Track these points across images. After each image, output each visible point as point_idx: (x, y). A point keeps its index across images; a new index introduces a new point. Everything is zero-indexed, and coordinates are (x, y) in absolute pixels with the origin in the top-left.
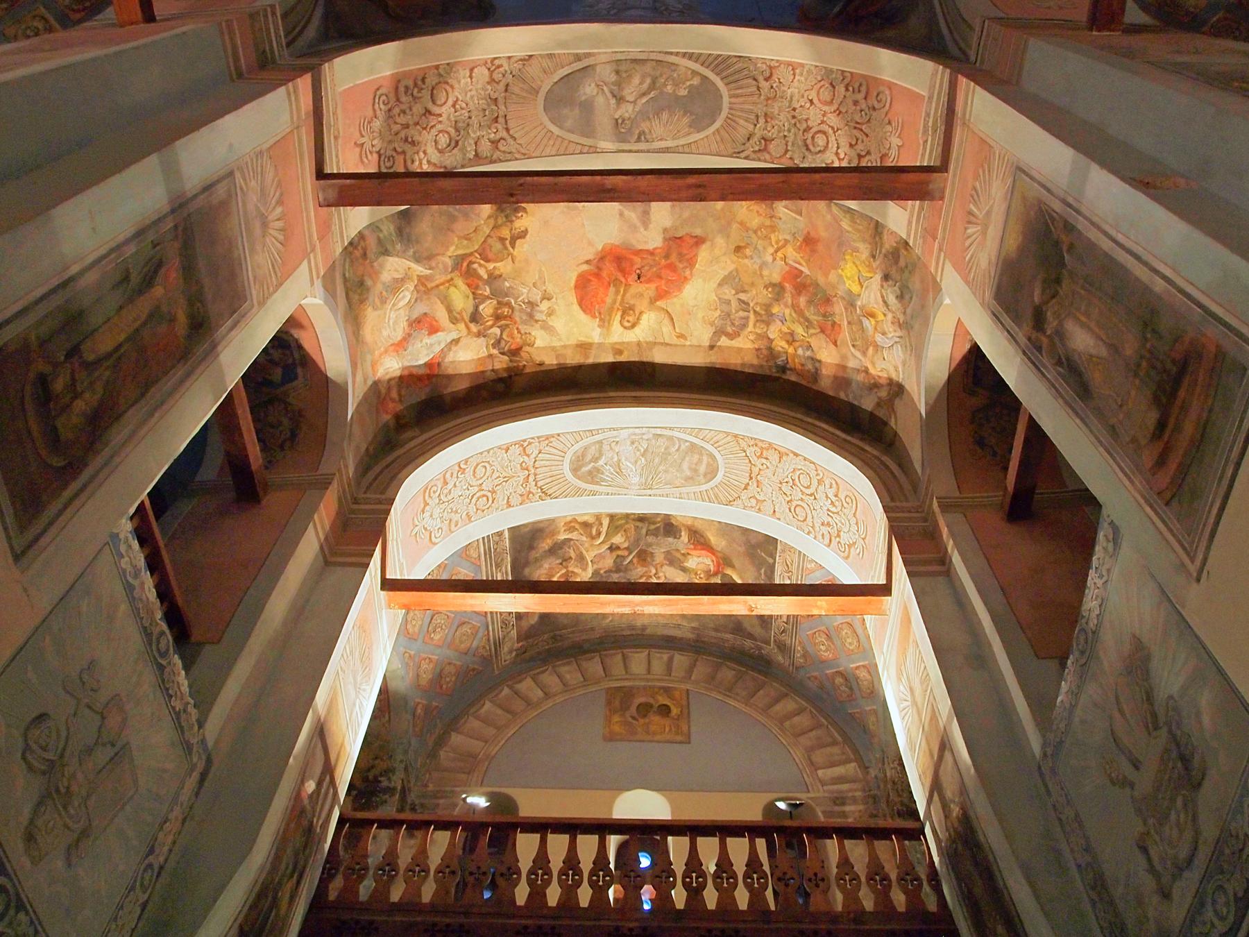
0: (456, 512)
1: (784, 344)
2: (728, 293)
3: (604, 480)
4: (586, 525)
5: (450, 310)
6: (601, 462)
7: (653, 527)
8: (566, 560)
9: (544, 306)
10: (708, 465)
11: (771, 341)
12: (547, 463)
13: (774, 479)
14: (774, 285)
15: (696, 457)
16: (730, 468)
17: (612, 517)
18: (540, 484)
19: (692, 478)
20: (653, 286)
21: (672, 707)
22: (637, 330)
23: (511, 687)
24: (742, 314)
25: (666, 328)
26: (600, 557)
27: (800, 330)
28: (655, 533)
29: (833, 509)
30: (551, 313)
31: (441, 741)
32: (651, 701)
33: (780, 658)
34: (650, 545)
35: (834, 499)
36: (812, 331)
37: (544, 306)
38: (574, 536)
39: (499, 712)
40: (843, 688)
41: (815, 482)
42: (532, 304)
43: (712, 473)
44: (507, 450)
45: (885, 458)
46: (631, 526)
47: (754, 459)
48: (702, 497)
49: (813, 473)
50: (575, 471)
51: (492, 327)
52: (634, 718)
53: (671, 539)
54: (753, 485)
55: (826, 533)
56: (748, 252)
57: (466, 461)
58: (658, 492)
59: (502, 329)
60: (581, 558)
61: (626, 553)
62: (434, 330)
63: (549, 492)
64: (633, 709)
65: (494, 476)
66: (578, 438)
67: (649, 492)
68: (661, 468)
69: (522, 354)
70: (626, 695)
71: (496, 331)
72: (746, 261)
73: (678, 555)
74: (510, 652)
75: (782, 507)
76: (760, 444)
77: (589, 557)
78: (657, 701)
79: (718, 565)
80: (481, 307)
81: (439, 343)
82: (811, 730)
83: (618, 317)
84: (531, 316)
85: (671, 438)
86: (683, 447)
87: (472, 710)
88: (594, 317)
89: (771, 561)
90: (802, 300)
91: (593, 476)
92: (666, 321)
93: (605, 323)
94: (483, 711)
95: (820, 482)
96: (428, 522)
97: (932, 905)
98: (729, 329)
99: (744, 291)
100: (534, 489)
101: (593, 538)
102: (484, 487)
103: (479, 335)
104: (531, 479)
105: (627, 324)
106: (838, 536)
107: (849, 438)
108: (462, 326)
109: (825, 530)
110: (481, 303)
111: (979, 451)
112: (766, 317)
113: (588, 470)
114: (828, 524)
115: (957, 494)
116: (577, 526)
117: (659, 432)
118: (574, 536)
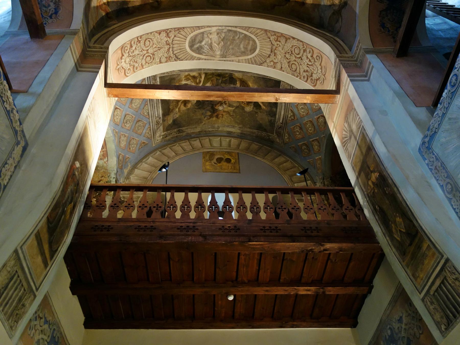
0: (136, 62)
3: (205, 53)
4: (194, 77)
6: (203, 43)
7: (224, 79)
10: (252, 45)
12: (178, 42)
15: (247, 41)
16: (262, 47)
18: (175, 52)
19: (244, 52)
21: (232, 159)
23: (160, 152)
28: (225, 82)
29: (310, 63)
32: (222, 157)
33: (278, 140)
35: (310, 58)
40: (306, 150)
41: (302, 51)
43: (254, 49)
44: (160, 33)
45: (336, 38)
46: (214, 78)
47: (274, 42)
50: (191, 47)
52: (215, 163)
63: (179, 57)
64: (215, 160)
65: (155, 46)
66: (193, 30)
67: (224, 59)
68: (231, 47)
70: (212, 155)
74: (160, 136)
75: (285, 65)
76: (277, 34)
78: (225, 157)
85: (235, 32)
86: (241, 36)
87: (144, 160)
91: (199, 50)
94: (148, 161)
95: (304, 51)
96: (123, 64)
100: (172, 55)
102: (149, 51)
104: (171, 50)
106: (312, 76)
109: (305, 74)
111: (382, 29)
116: (190, 78)
117: (230, 28)
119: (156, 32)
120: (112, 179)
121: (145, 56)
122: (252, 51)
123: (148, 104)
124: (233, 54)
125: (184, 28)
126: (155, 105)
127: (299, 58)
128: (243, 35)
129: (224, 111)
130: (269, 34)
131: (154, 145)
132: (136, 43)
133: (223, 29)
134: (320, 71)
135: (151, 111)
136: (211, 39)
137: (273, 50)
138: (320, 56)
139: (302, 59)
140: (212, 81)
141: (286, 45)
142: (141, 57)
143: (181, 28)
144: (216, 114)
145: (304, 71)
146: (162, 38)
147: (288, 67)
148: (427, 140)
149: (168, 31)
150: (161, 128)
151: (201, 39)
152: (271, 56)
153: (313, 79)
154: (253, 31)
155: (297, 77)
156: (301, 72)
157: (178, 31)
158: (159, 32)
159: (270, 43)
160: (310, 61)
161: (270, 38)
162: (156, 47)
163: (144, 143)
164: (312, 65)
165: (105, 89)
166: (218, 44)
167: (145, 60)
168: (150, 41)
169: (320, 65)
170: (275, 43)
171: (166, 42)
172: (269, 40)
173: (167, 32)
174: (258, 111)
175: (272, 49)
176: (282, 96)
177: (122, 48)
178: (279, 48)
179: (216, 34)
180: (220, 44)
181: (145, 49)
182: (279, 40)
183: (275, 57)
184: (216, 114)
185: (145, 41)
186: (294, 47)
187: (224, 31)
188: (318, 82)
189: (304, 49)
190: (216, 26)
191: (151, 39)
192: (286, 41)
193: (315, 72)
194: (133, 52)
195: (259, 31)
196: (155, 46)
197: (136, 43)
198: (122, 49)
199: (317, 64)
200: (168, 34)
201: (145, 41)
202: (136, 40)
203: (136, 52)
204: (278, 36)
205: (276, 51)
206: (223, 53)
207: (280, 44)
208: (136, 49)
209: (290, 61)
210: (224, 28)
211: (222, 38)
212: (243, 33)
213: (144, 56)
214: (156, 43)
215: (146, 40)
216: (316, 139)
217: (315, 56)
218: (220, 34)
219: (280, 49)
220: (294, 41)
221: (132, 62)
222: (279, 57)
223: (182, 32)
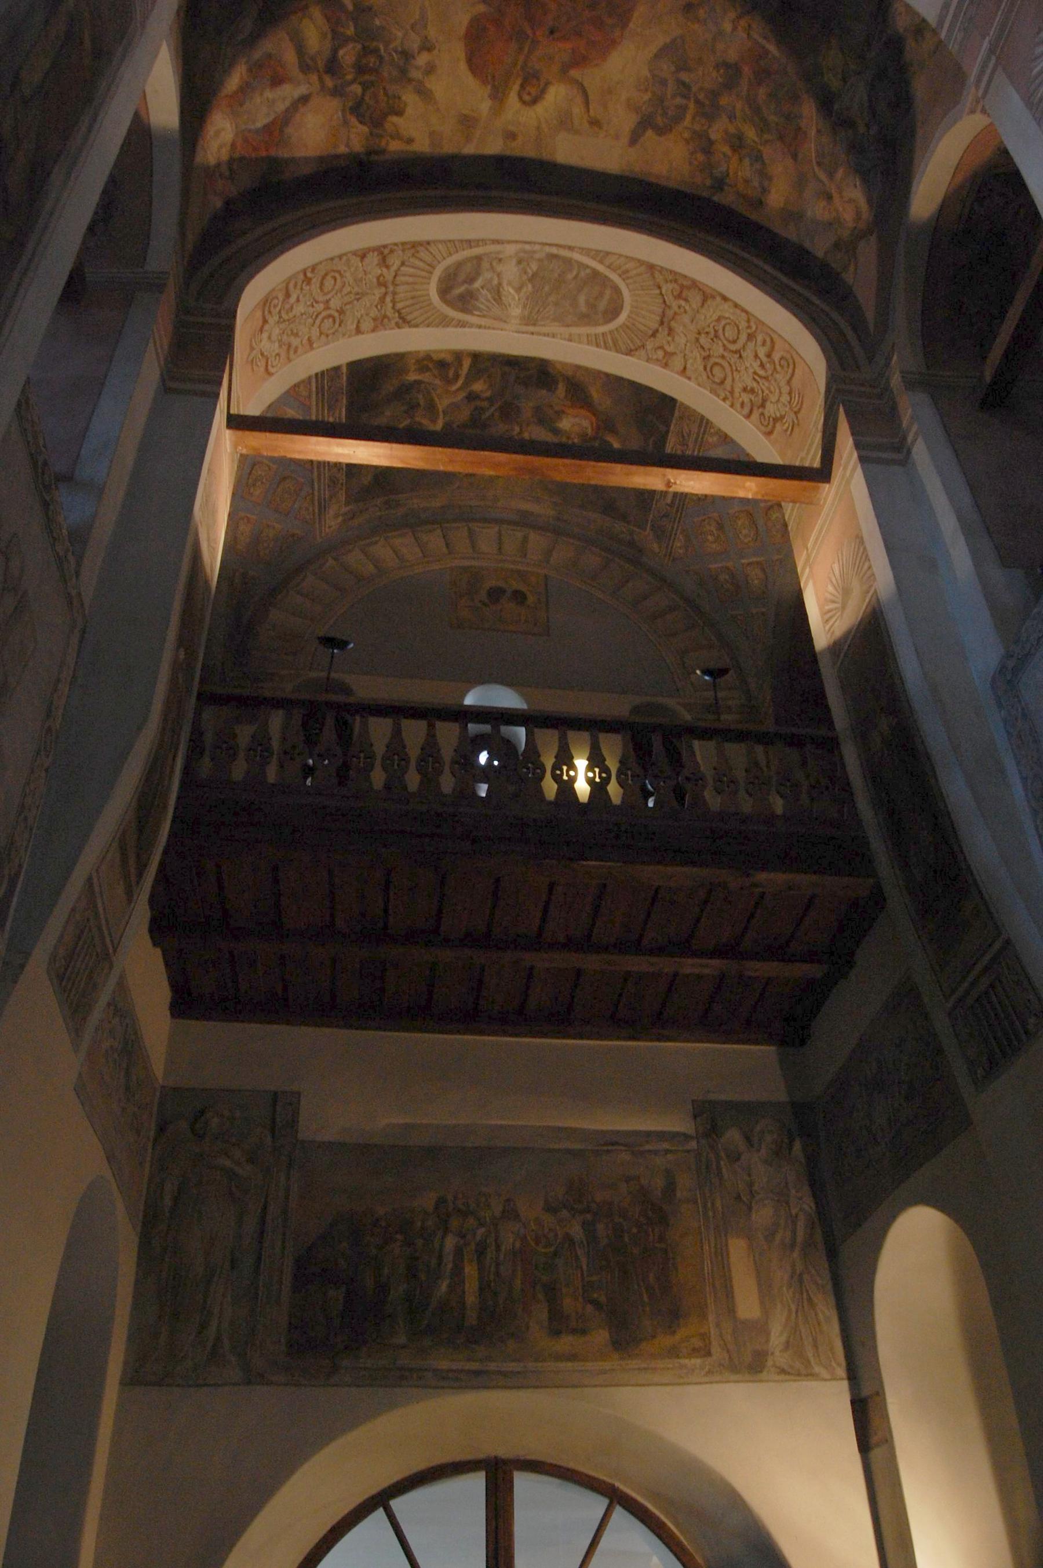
0: (296, 335)
1: (726, 149)
2: (666, 68)
3: (479, 309)
4: (442, 365)
5: (300, 50)
6: (477, 284)
8: (413, 407)
9: (422, 59)
11: (711, 143)
12: (411, 280)
14: (727, 65)
17: (476, 356)
18: (399, 306)
20: (568, 46)
21: (528, 594)
22: (539, 108)
23: (335, 559)
24: (679, 101)
25: (577, 110)
26: (455, 406)
27: (751, 134)
29: (762, 373)
30: (430, 69)
32: (501, 584)
33: (655, 546)
35: (764, 359)
36: (766, 136)
37: (422, 59)
38: (426, 377)
41: (743, 337)
42: (407, 55)
43: (613, 312)
44: (363, 257)
47: (670, 299)
48: (597, 341)
49: (743, 325)
51: (353, 81)
54: (663, 333)
55: (746, 400)
56: (702, 13)
57: (313, 268)
58: (545, 330)
59: (365, 86)
60: (431, 407)
61: (485, 404)
62: (277, 81)
63: (409, 318)
64: (483, 594)
67: (531, 329)
68: (551, 299)
69: (387, 125)
71: (357, 89)
72: (696, 26)
74: (336, 516)
75: (696, 363)
77: (442, 404)
79: (598, 428)
80: (341, 53)
81: (284, 99)
83: (516, 87)
84: (403, 71)
85: (568, 261)
86: (582, 274)
88: (484, 82)
90: (762, 92)
91: (465, 302)
92: (579, 99)
93: (498, 96)
95: (751, 337)
96: (265, 345)
98: (660, 120)
99: (688, 70)
100: (390, 312)
101: (449, 382)
102: (332, 304)
103: (336, 92)
104: (388, 299)
105: (527, 98)
106: (763, 406)
107: (792, 284)
108: (314, 78)
109: (746, 397)
110: (341, 46)
112: (709, 110)
113: (461, 291)
114: (752, 391)
117: (554, 250)
118: (426, 377)
119: (354, 253)
121: (320, 317)
125: (428, 243)
127: (736, 352)
128: (588, 271)
131: (319, 540)
132: (299, 287)
133: (534, 252)
134: (785, 398)
136: (499, 275)
137: (666, 320)
138: (791, 361)
139: (741, 356)
140: (489, 377)
142: (310, 320)
143: (420, 244)
145: (745, 390)
147: (701, 368)
148: (1011, 664)
149: (386, 251)
150: (342, 496)
152: (658, 335)
153: (767, 414)
156: (737, 390)
157: (413, 251)
159: (661, 301)
160: (762, 365)
161: (659, 288)
162: (350, 292)
163: (293, 535)
164: (766, 378)
165: (228, 431)
166: (518, 290)
167: (320, 327)
169: (789, 382)
170: (674, 304)
171: (378, 278)
172: (658, 291)
173: (382, 253)
175: (664, 314)
176: (683, 476)
177: (266, 303)
179: (514, 262)
180: (524, 290)
181: (321, 298)
182: (684, 294)
183: (669, 339)
185: (324, 278)
186: (723, 322)
187: (537, 256)
188: (778, 425)
190: (516, 242)
191: (339, 272)
192: (704, 301)
193: (774, 399)
194: (292, 308)
195: (630, 265)
197: (299, 287)
198: (265, 304)
199: (781, 378)
200: (384, 259)
201: (324, 278)
202: (302, 276)
203: (300, 309)
204: (682, 287)
205: (673, 324)
207: (687, 308)
208: (298, 300)
209: (709, 356)
210: (537, 247)
212: (588, 267)
213: (317, 316)
214: (351, 281)
215: (326, 274)
216: (758, 563)
217: (776, 356)
220: (726, 306)
221: (285, 337)
222: (681, 340)
223: (423, 254)
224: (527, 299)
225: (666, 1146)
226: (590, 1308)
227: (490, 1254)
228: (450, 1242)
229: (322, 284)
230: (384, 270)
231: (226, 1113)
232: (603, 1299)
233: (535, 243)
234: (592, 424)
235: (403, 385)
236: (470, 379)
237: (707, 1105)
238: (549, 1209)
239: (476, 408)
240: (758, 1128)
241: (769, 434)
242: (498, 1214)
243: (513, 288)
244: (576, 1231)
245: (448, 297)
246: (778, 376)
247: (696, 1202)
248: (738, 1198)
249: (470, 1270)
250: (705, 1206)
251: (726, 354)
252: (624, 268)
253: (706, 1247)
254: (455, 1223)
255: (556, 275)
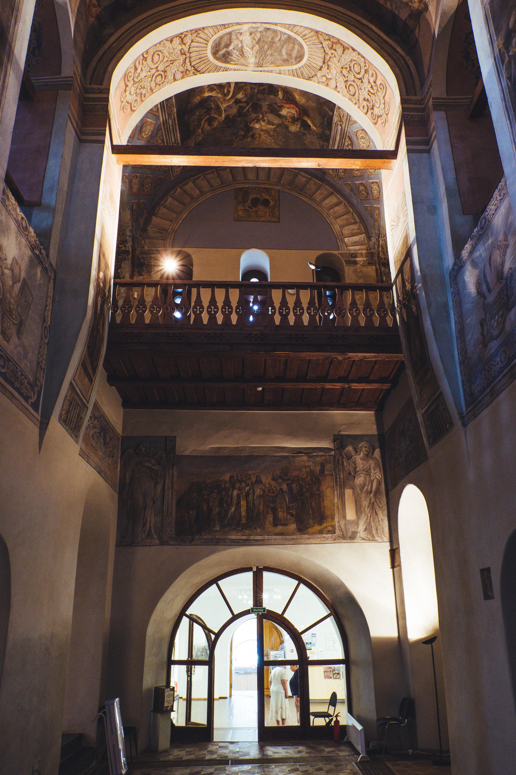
0: (144, 88)
3: (232, 60)
6: (231, 48)
8: (209, 109)
10: (298, 51)
12: (197, 49)
13: (338, 65)
15: (291, 45)
16: (311, 55)
17: (236, 83)
18: (193, 63)
21: (271, 201)
23: (181, 188)
26: (229, 107)
31: (148, 222)
32: (259, 196)
34: (259, 100)
35: (373, 84)
38: (213, 94)
39: (177, 203)
40: (363, 192)
41: (363, 71)
43: (300, 57)
44: (171, 41)
45: (407, 58)
47: (327, 50)
49: (363, 65)
50: (215, 53)
52: (249, 207)
53: (272, 97)
54: (325, 67)
55: (365, 105)
57: (147, 52)
60: (218, 108)
61: (245, 105)
63: (199, 69)
64: (249, 202)
65: (165, 60)
66: (216, 31)
67: (260, 69)
68: (269, 52)
70: (245, 192)
73: (276, 107)
75: (341, 85)
77: (223, 106)
79: (300, 114)
82: (343, 215)
85: (275, 31)
86: (283, 38)
87: (162, 202)
89: (331, 113)
91: (226, 58)
94: (167, 203)
95: (366, 71)
97: (390, 324)
100: (189, 68)
102: (159, 69)
104: (187, 61)
106: (372, 109)
107: (388, 39)
109: (365, 103)
113: (223, 53)
115: (445, 96)
117: (268, 26)
118: (213, 94)
120: (127, 238)
121: (154, 76)
122: (298, 59)
123: (161, 129)
124: (272, 63)
125: (203, 28)
126: (171, 128)
128: (286, 36)
129: (262, 130)
130: (321, 38)
131: (173, 179)
132: (141, 63)
133: (258, 28)
134: (382, 106)
135: (166, 136)
136: (241, 41)
138: (385, 86)
139: (362, 82)
140: (245, 90)
141: (343, 56)
142: (150, 79)
144: (251, 133)
145: (364, 99)
146: (175, 47)
147: (344, 87)
151: (228, 43)
152: (322, 69)
153: (374, 113)
154: (299, 31)
155: (356, 104)
156: (361, 99)
157: (196, 34)
158: (170, 39)
159: (323, 51)
160: (372, 87)
161: (322, 44)
162: (167, 61)
163: (160, 178)
164: (374, 94)
165: (114, 156)
167: (155, 81)
168: (158, 54)
170: (329, 52)
171: (181, 51)
172: (321, 46)
173: (181, 37)
174: (306, 132)
175: (324, 59)
177: (126, 76)
178: (335, 59)
179: (248, 34)
180: (255, 48)
182: (334, 48)
183: (329, 71)
184: (251, 133)
185: (153, 56)
186: (353, 63)
187: (259, 30)
188: (379, 119)
189: (366, 68)
191: (160, 51)
192: (344, 50)
195: (307, 31)
196: (165, 60)
197: (141, 63)
198: (125, 77)
199: (381, 94)
200: (182, 40)
201: (153, 56)
202: (142, 58)
204: (333, 42)
206: (259, 61)
208: (142, 70)
210: (259, 25)
211: (257, 39)
212: (285, 34)
213: (153, 77)
214: (168, 55)
215: (154, 54)
216: (376, 182)
217: (378, 83)
218: (253, 35)
219: (336, 61)
220: (355, 54)
221: (138, 90)
222: (334, 71)
224: (257, 53)
225: (322, 453)
226: (289, 516)
227: (250, 497)
228: (235, 493)
229: (152, 58)
230: (183, 46)
231: (148, 446)
232: (294, 513)
233: (257, 23)
234: (297, 111)
235: (203, 98)
236: (235, 94)
237: (340, 437)
238: (274, 479)
239: (240, 107)
240: (360, 445)
241: (375, 124)
242: (254, 482)
243: (249, 48)
244: (285, 487)
245: (217, 55)
246: (379, 93)
247: (332, 475)
248: (350, 473)
249: (243, 503)
250: (336, 478)
251: (355, 80)
252: (304, 33)
253: (336, 493)
254: (237, 485)
255: (270, 39)
